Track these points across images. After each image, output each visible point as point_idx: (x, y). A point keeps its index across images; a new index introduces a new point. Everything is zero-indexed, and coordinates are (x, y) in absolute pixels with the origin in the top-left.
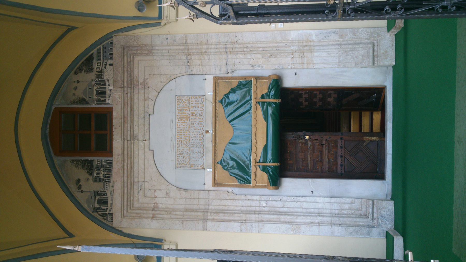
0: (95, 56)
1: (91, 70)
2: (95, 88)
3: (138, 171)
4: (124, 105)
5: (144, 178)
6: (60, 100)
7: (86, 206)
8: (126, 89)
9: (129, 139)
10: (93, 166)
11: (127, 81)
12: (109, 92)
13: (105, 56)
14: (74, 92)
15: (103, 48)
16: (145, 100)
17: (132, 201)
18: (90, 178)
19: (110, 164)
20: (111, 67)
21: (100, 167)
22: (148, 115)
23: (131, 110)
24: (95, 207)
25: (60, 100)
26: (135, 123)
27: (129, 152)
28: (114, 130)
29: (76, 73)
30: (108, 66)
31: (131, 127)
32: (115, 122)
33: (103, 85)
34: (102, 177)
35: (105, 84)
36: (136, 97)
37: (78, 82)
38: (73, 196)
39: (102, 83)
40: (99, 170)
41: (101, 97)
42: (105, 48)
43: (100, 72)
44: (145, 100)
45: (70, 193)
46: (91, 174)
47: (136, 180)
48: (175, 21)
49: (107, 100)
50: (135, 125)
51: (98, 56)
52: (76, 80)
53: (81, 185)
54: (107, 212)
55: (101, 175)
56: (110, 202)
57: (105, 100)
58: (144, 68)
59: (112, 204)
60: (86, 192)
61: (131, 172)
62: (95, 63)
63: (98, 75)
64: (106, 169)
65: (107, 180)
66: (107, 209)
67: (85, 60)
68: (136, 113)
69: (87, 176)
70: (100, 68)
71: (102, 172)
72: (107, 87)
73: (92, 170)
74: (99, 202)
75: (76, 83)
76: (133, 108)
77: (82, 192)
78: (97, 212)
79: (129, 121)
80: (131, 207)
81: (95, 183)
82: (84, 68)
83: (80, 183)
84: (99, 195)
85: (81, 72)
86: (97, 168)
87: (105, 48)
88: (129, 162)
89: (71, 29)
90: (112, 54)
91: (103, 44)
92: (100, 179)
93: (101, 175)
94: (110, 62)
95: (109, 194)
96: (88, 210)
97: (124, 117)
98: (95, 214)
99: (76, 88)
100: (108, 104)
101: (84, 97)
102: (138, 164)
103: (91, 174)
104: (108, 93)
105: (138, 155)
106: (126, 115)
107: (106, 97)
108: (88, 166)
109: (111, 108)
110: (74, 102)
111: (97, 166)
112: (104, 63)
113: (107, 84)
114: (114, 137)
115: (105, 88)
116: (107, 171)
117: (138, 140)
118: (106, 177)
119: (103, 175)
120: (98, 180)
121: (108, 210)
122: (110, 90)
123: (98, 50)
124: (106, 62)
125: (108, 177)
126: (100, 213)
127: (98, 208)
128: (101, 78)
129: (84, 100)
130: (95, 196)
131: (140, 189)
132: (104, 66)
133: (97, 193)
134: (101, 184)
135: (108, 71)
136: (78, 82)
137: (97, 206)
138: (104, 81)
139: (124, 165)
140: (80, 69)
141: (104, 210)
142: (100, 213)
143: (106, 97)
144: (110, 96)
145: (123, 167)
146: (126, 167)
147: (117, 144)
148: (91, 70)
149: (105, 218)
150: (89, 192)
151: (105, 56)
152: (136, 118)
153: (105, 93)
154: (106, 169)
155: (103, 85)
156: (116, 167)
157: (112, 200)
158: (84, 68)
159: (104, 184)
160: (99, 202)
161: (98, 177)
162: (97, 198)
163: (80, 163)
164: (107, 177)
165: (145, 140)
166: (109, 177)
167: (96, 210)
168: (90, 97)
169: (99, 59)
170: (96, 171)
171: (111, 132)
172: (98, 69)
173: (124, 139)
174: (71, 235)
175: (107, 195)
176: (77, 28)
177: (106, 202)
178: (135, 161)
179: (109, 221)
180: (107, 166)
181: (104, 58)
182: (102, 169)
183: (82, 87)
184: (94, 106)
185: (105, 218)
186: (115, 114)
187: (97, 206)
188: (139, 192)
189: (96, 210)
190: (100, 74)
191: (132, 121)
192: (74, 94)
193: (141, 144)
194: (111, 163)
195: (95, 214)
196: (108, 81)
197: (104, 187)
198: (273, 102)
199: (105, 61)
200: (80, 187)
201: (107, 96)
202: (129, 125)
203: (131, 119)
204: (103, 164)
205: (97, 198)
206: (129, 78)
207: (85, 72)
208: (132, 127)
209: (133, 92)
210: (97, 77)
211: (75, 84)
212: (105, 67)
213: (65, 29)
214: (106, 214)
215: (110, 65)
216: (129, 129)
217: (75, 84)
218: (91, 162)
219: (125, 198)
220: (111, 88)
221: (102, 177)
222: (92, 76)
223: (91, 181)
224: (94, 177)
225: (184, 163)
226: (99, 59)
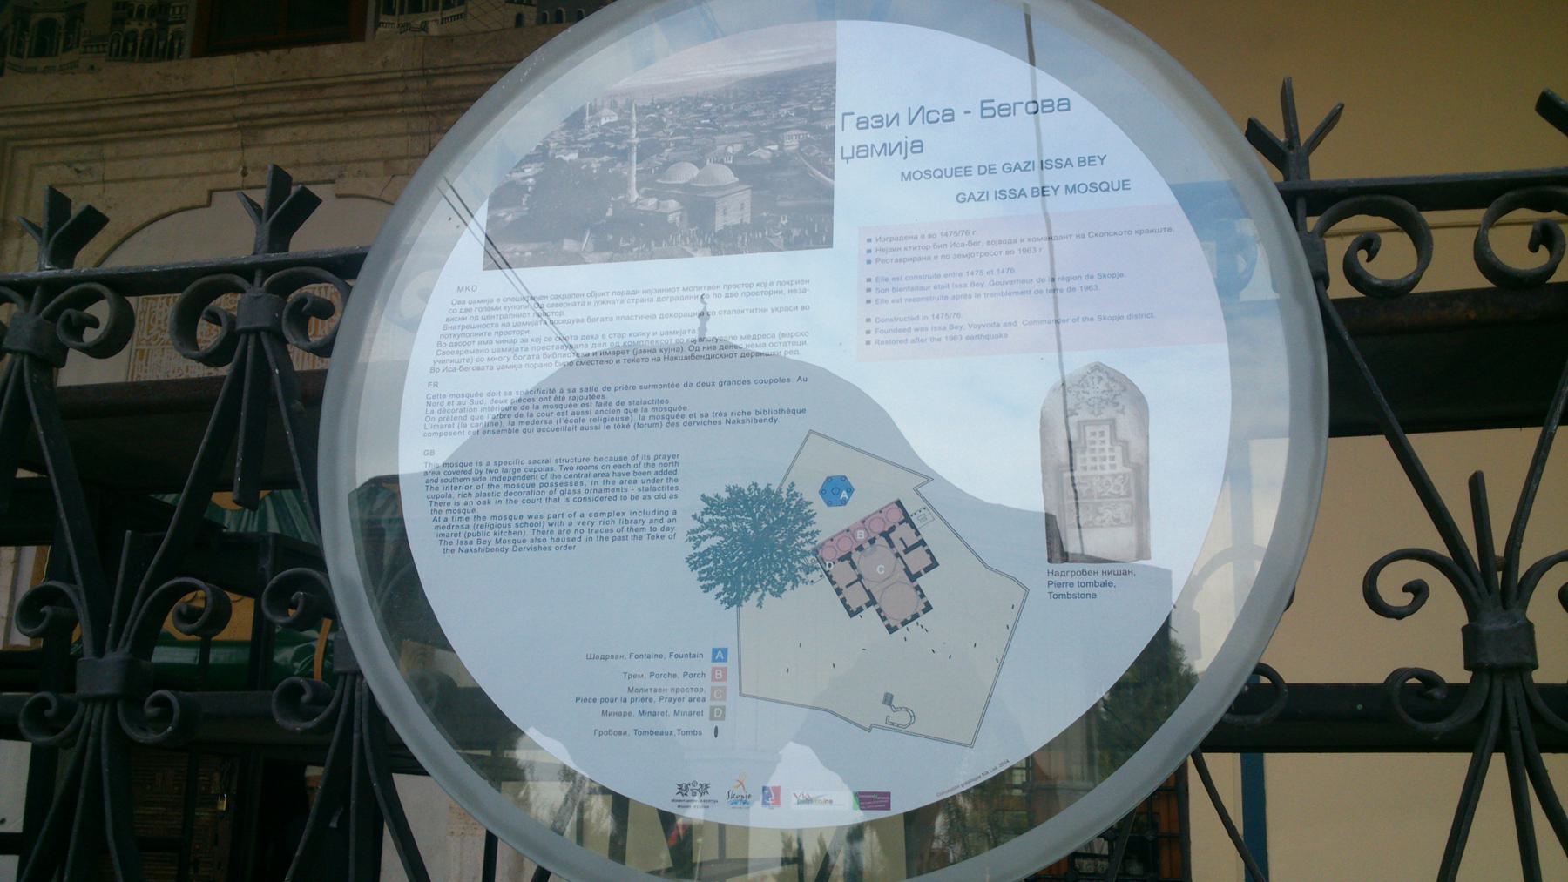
3: (137, 158)
4: (365, 83)
5: (116, 181)
8: (422, 84)
9: (240, 113)
11: (451, 88)
16: (387, 161)
17: (34, 142)
19: (170, 54)
20: (511, 22)
22: (332, 175)
23: (346, 111)
26: (303, 131)
27: (194, 118)
28: (275, 53)
30: (513, 10)
31: (281, 114)
32: (303, 53)
34: (128, 28)
36: (397, 125)
44: (387, 161)
47: (109, 151)
49: (390, 19)
50: (295, 130)
55: (133, 25)
56: (43, 63)
57: (389, 10)
59: (33, 70)
61: (132, 130)
66: (20, 56)
68: (338, 129)
71: (146, 25)
76: (354, 119)
79: (300, 107)
80: (14, 139)
88: (160, 120)
94: (530, 13)
95: (67, 58)
97: (321, 87)
100: (377, 24)
102: (164, 155)
104: (417, 20)
105: (192, 152)
106: (328, 92)
107: (402, 12)
113: (448, 13)
114: (251, 56)
115: (435, 9)
117: (243, 147)
118: (126, 40)
119: (134, 32)
121: (16, 61)
122: (424, 28)
125: (124, 50)
131: (81, 168)
139: (155, 102)
142: (11, 32)
143: (402, 12)
144: (406, 27)
145: (145, 100)
146: (150, 109)
147: (227, 70)
152: (321, 131)
156: (149, 75)
157: (47, 70)
161: (130, 15)
162: (60, 18)
165: (244, 174)
166: (125, 52)
171: (267, 46)
173: (244, 94)
175: (64, 51)
177: (42, 50)
178: (172, 142)
180: (161, 44)
182: (155, 25)
186: (329, 51)
188: (69, 164)
191: (306, 118)
193: (232, 160)
194: (171, 57)
196: (459, 16)
198: (311, 665)
202: (286, 108)
203: (309, 113)
204: (172, 28)
205: (60, 18)
206: (457, 94)
208: (283, 120)
209: (413, 115)
215: (519, 20)
216: (274, 109)
219: (47, 118)
220: (434, 29)
221: (128, 28)
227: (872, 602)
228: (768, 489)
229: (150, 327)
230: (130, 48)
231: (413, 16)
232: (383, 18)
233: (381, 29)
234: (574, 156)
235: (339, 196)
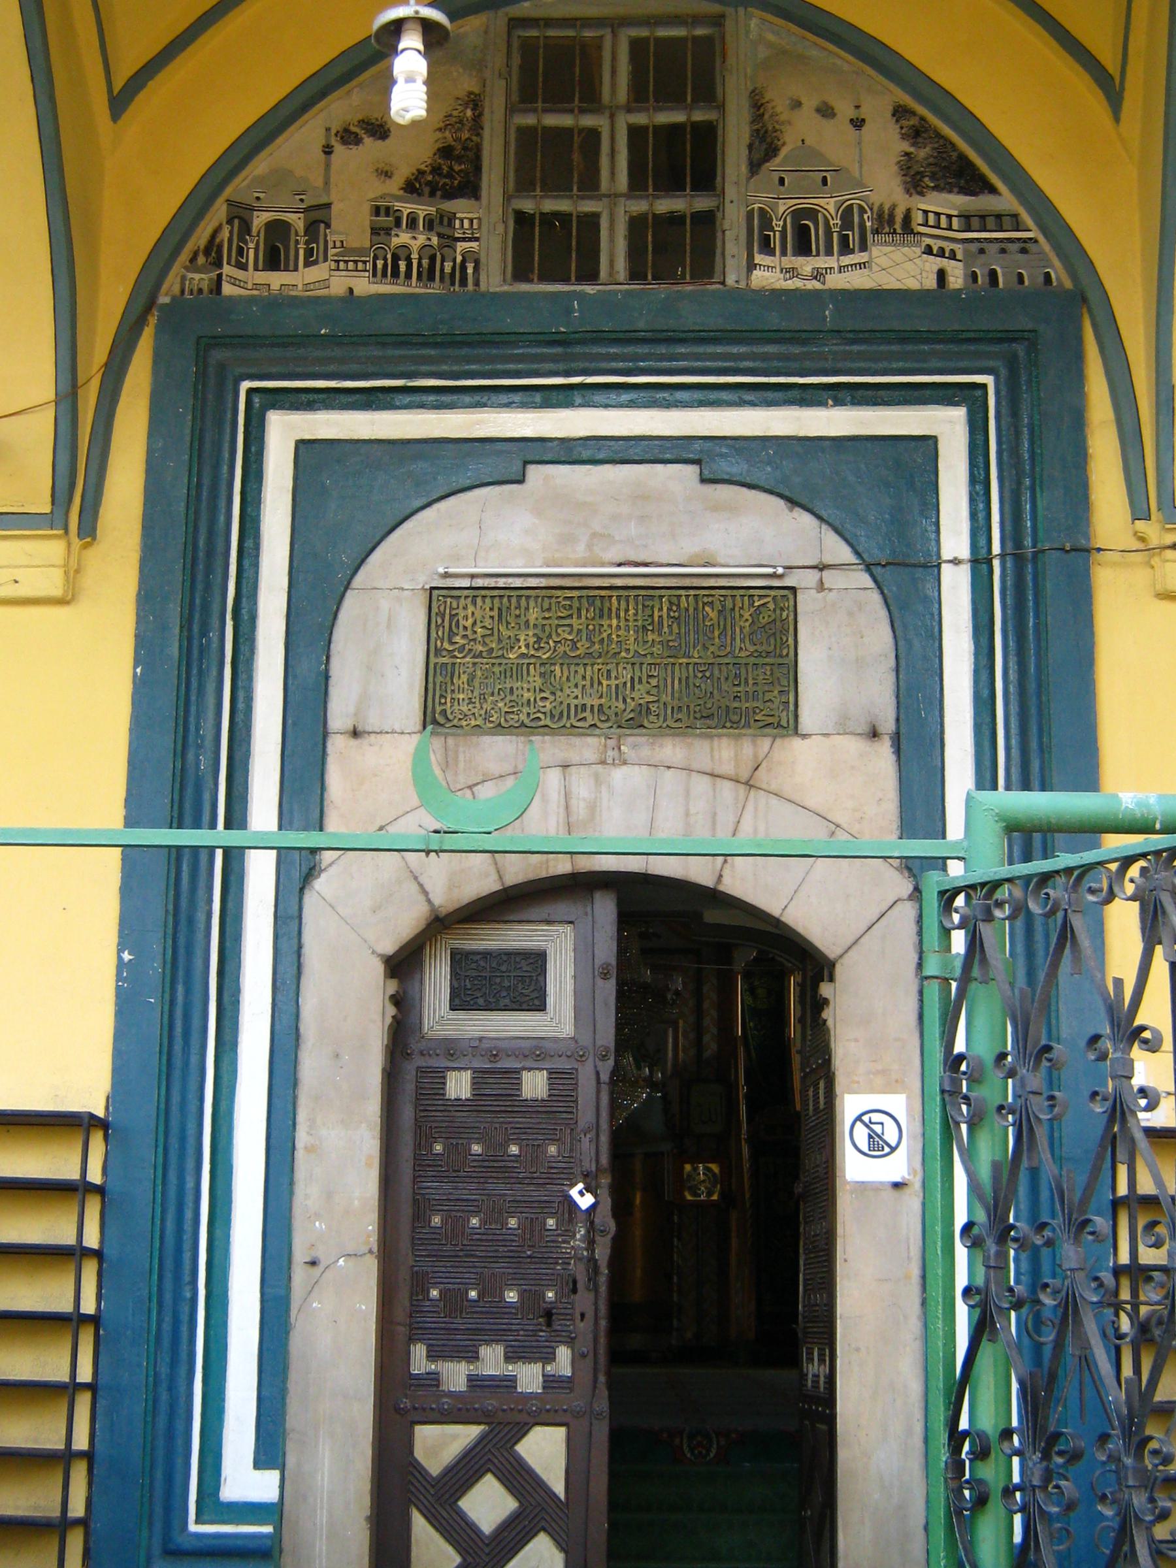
0: (985, 203)
1: (915, 183)
2: (829, 205)
6: (771, 37)
7: (260, 166)
10: (449, 195)
12: (807, 270)
13: (982, 251)
14: (810, 103)
15: (1025, 240)
18: (394, 186)
21: (445, 230)
24: (252, 209)
25: (771, 37)
29: (900, 112)
30: (934, 264)
33: (844, 240)
34: (395, 241)
35: (845, 249)
37: (858, 123)
38: (305, 107)
39: (854, 237)
40: (430, 225)
41: (784, 233)
42: (1025, 247)
45: (323, 94)
46: (411, 188)
48: (1158, 587)
51: (983, 217)
52: (864, 112)
53: (358, 141)
54: (227, 269)
55: (402, 238)
57: (766, 247)
60: (328, 165)
62: (949, 203)
63: (892, 216)
64: (432, 259)
65: (380, 263)
66: (243, 267)
67: (963, 157)
69: (404, 172)
70: (926, 224)
71: (422, 239)
72: (831, 262)
73: (432, 194)
74: (278, 229)
75: (851, 113)
77: (328, 150)
78: (230, 222)
81: (366, 209)
82: (922, 153)
83: (368, 140)
84: (312, 229)
85: (904, 137)
86: (441, 215)
87: (1024, 251)
89: (1112, 90)
91: (1041, 239)
92: (388, 231)
93: (402, 238)
96: (237, 181)
98: (219, 212)
99: (826, 111)
101: (783, 152)
103: (411, 188)
107: (784, 253)
108: (450, 176)
110: (758, 105)
111: (452, 217)
112: (948, 246)
113: (846, 260)
115: (829, 252)
116: (425, 262)
118: (396, 258)
120: (384, 220)
123: (1015, 216)
124: (953, 256)
126: (225, 233)
127: (246, 228)
128: (876, 232)
129: (772, 151)
130: (306, 210)
132: (936, 245)
133: (318, 218)
134: (361, 238)
135: (909, 266)
136: (858, 123)
137: (260, 220)
138: (864, 247)
140: (918, 133)
141: (240, 252)
142: (225, 233)
143: (784, 253)
148: (915, 183)
149: (201, 260)
150: (327, 183)
151: (982, 251)
153: (803, 247)
154: (432, 259)
155: (844, 240)
158: (922, 153)
159: (361, 251)
160: (278, 229)
161: (398, 223)
162: (298, 222)
163: (465, 135)
164: (396, 267)
166: (396, 273)
167: (240, 215)
168: (782, 181)
169: (968, 222)
170: (423, 211)
172: (918, 217)
174: (119, 103)
175: (307, 264)
176: (1117, 119)
179: (183, 278)
180: (448, 267)
181: (974, 247)
182: (435, 240)
183: (832, 141)
185: (201, 260)
187: (260, 220)
189: (240, 215)
190: (895, 226)
192: (797, 104)
195: (219, 212)
196: (862, 265)
197: (346, 250)
199: (958, 248)
200: (349, 137)
201: (791, 261)
205: (298, 222)
207: (907, 154)
210: (880, 215)
211: (845, 110)
212: (929, 251)
213: (1108, 58)
214: (220, 266)
217: (845, 110)
218: (470, 188)
221: (395, 241)
222: (885, 188)
223: (376, 189)
224: (398, 205)
225: (462, 632)
226: (968, 222)
229: (452, 634)
230: (402, 265)
231: (801, 259)
232: (758, 258)
233: (757, 273)
235: (704, 481)
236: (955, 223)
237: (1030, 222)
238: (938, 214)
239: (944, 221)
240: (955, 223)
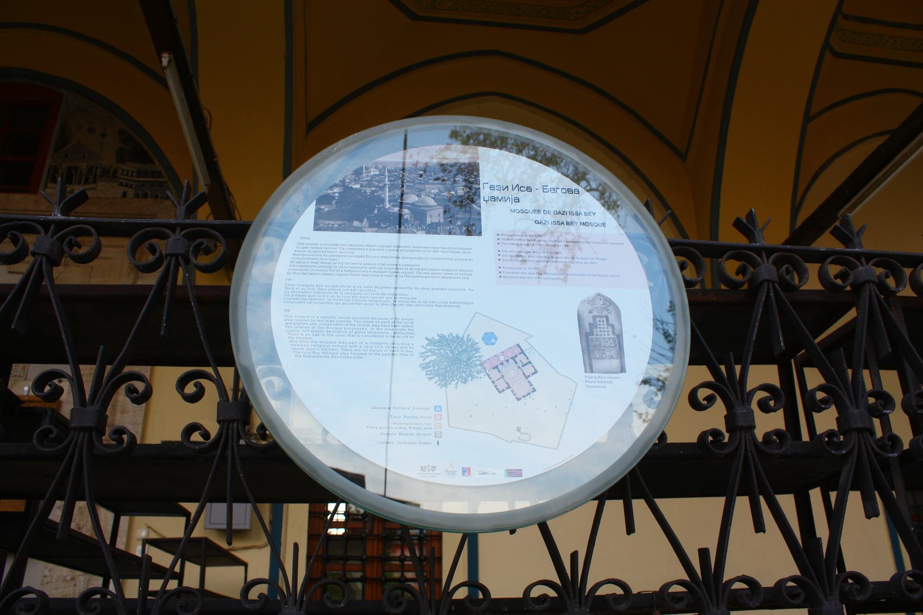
2: (84, 166)
30: (122, 189)
43: (114, 175)
49: (53, 185)
58: (109, 258)
70: (122, 174)
90: (146, 196)
94: (131, 193)
100: (46, 187)
109: (35, 192)
115: (79, 183)
124: (131, 187)
132: (124, 182)
136: (103, 136)
138: (94, 182)
168: (66, 156)
184: (49, 162)
186: (17, 197)
190: (109, 174)
196: (92, 189)
212: (121, 184)
215: (124, 195)
226: (140, 173)
227: (509, 387)
228: (457, 336)
233: (48, 190)
234: (358, 186)
236: (134, 174)
237: (165, 174)
238: (128, 171)
239: (130, 173)
240: (134, 174)
